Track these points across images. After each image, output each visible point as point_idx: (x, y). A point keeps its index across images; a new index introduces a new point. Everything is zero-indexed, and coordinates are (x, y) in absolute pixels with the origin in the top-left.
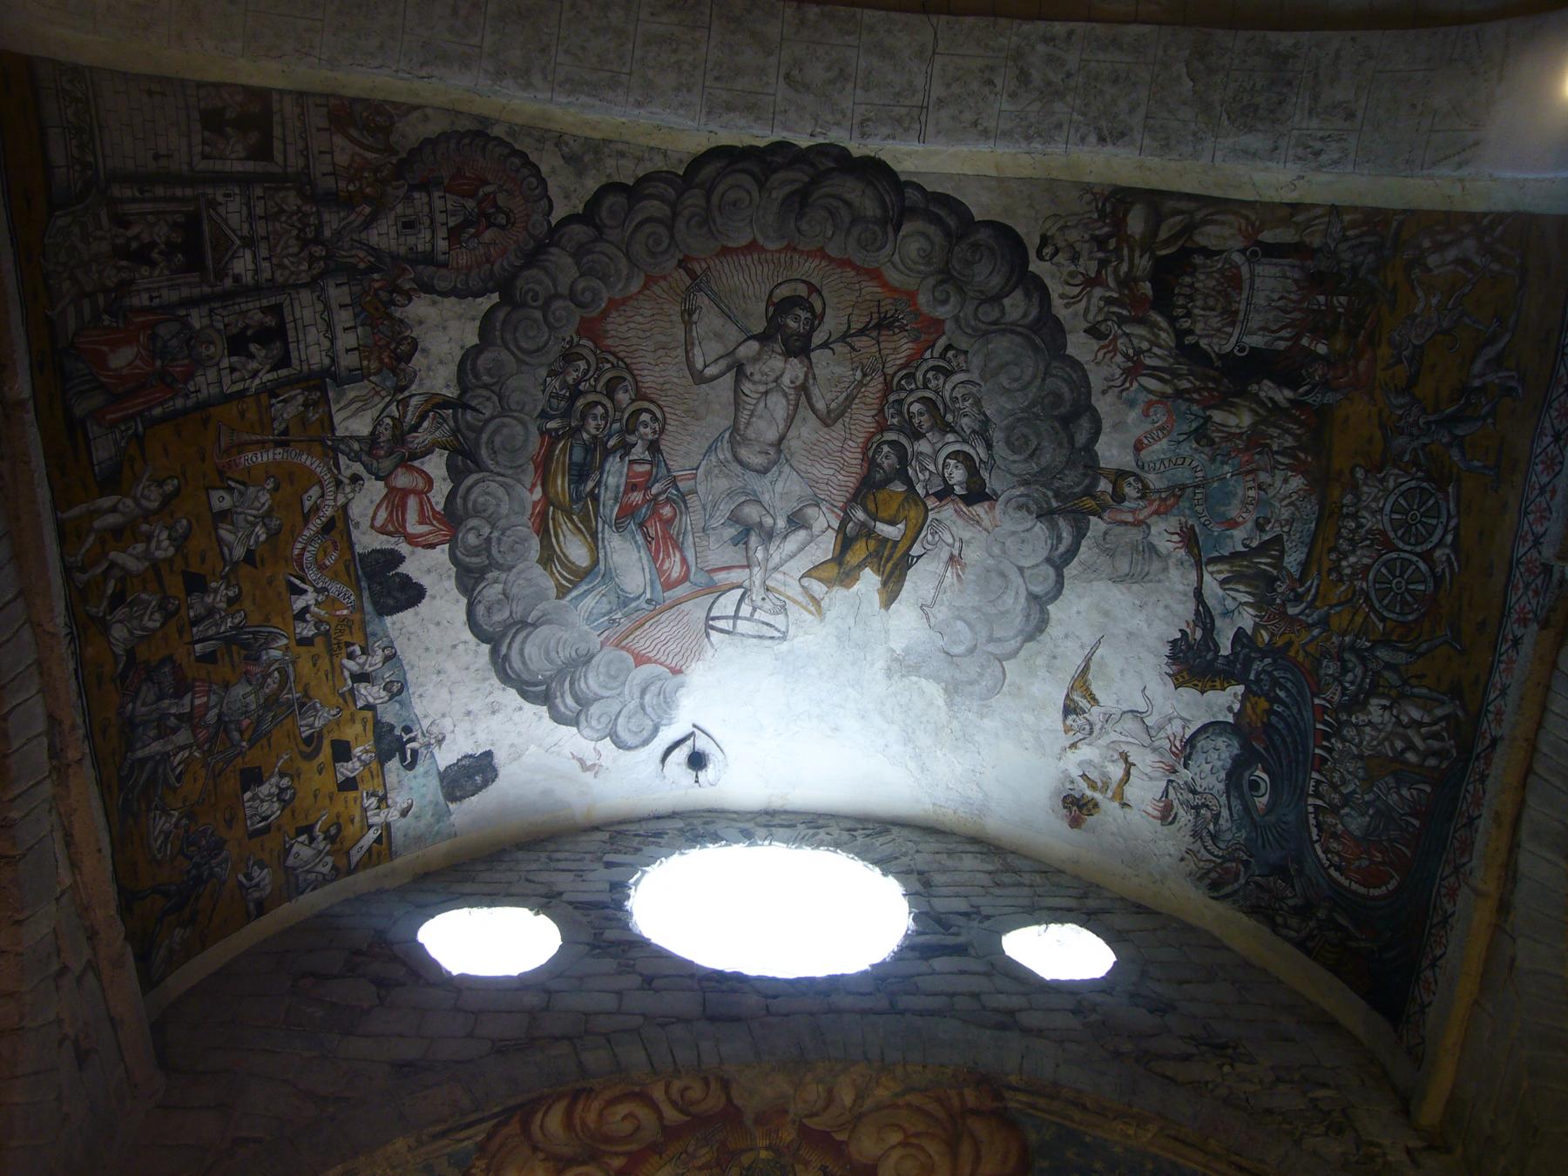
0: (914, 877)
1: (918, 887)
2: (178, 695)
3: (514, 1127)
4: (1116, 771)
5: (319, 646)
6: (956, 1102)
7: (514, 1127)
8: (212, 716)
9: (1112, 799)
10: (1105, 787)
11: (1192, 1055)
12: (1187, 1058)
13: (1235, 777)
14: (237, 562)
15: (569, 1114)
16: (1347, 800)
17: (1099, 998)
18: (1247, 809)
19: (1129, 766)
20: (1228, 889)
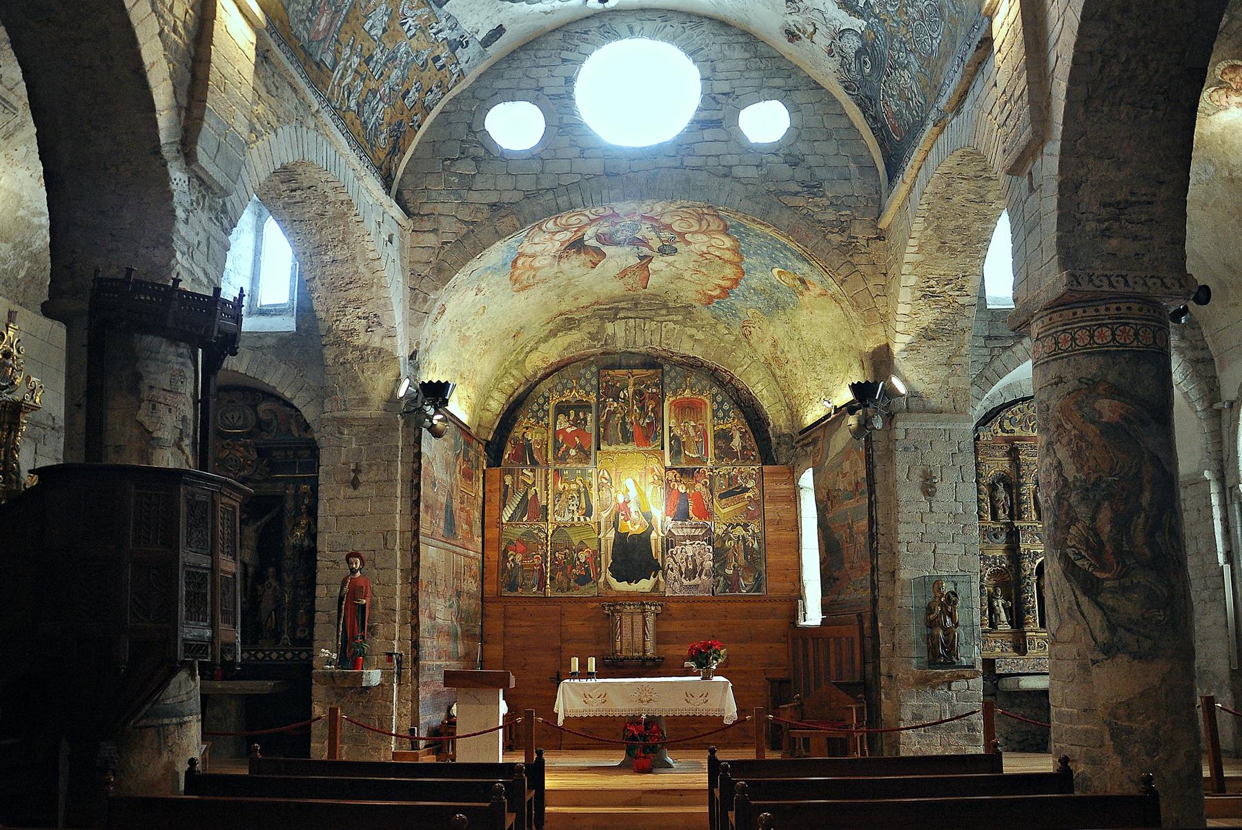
0: (709, 63)
1: (708, 73)
2: (375, 97)
3: (536, 229)
4: (811, 29)
5: (419, 33)
6: (700, 212)
7: (536, 229)
8: (387, 90)
9: (808, 38)
10: (804, 33)
11: (800, 192)
12: (796, 194)
13: (859, 53)
14: (380, 39)
15: (555, 222)
16: (893, 96)
17: (771, 158)
18: (861, 70)
19: (815, 29)
20: (851, 92)
